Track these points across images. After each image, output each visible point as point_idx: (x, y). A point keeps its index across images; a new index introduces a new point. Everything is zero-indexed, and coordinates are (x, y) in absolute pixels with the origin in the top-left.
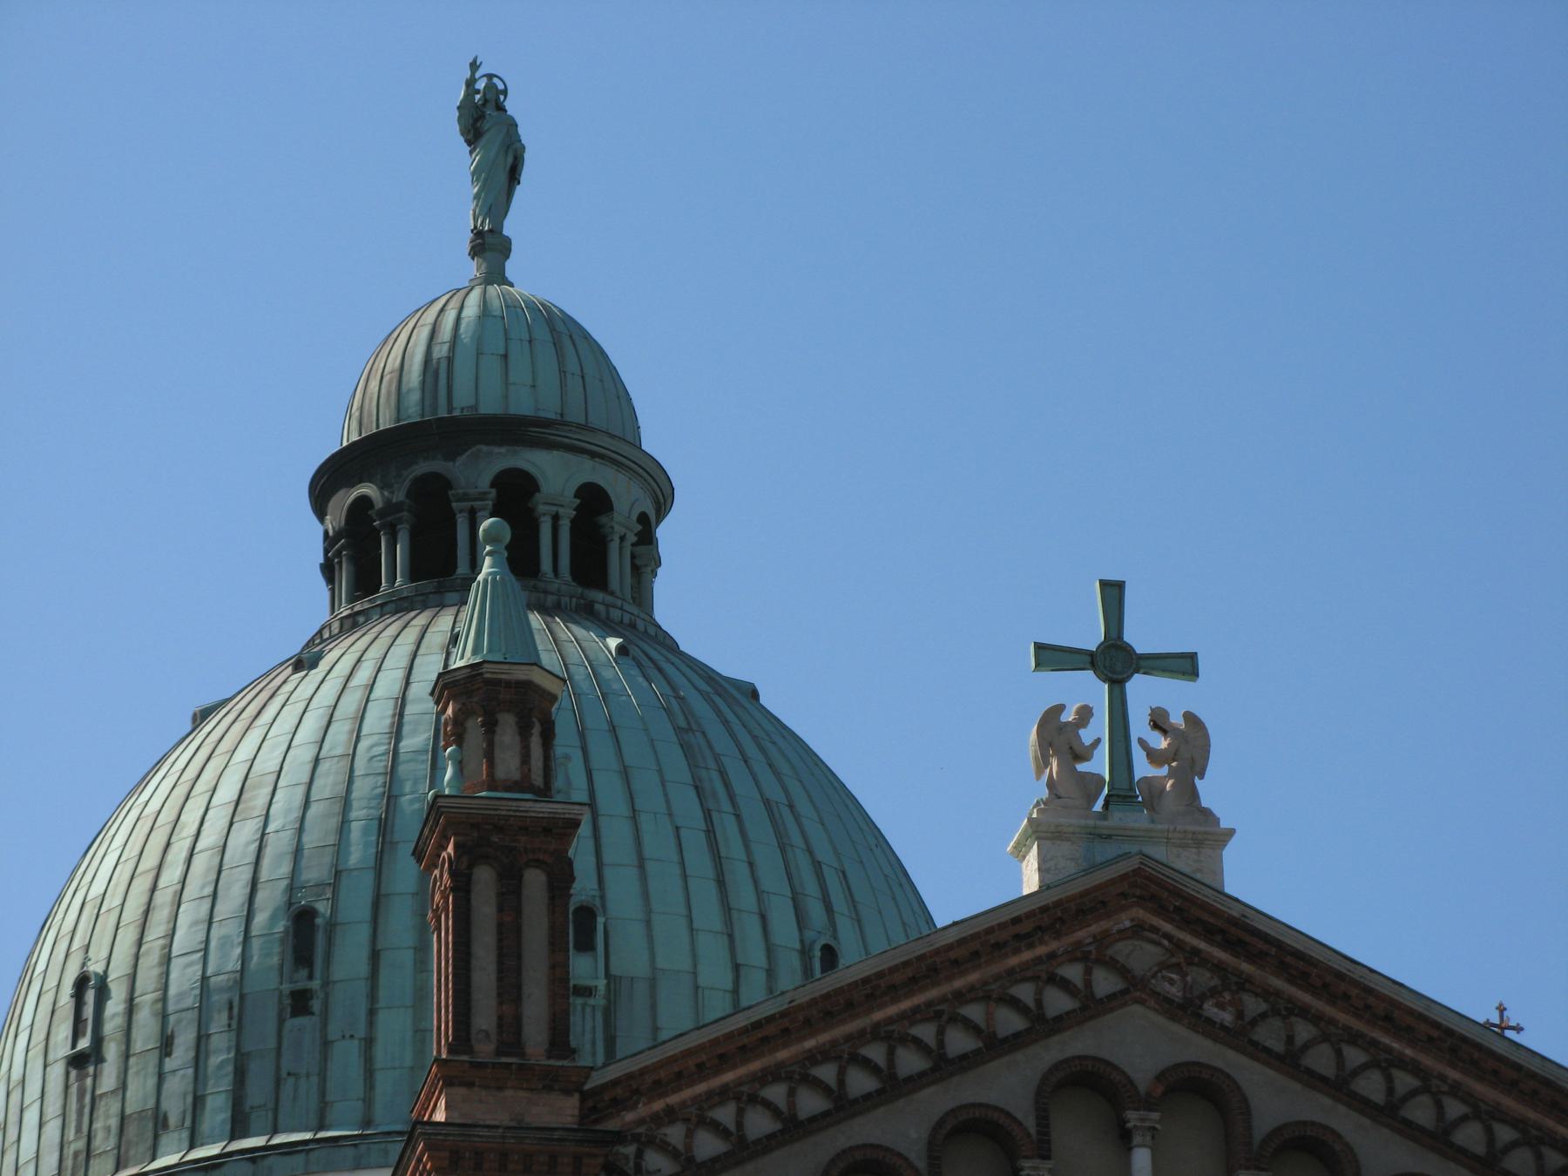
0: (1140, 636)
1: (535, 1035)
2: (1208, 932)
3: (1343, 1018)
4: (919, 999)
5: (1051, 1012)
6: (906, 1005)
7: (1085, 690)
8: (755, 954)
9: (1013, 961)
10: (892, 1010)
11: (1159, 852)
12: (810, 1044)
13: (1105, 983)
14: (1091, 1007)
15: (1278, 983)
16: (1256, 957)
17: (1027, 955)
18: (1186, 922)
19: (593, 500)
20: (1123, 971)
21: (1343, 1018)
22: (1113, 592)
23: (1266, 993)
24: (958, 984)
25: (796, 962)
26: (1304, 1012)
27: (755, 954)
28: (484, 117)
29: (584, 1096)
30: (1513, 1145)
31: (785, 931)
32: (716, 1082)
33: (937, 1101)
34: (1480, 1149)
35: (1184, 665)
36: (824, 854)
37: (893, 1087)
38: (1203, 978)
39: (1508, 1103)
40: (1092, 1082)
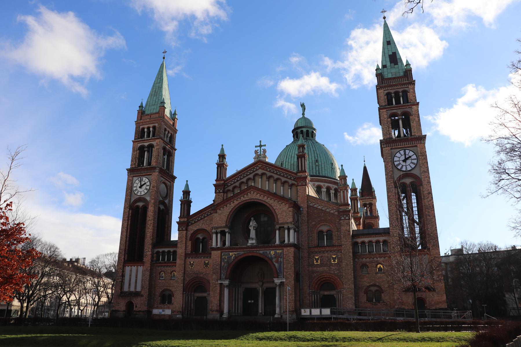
0: (262, 144)
7: (259, 148)
8: (311, 161)
11: (262, 159)
13: (258, 168)
14: (257, 170)
19: (307, 131)
22: (260, 141)
27: (311, 161)
28: (303, 106)
31: (313, 159)
33: (247, 177)
35: (265, 145)
36: (318, 153)
37: (244, 177)
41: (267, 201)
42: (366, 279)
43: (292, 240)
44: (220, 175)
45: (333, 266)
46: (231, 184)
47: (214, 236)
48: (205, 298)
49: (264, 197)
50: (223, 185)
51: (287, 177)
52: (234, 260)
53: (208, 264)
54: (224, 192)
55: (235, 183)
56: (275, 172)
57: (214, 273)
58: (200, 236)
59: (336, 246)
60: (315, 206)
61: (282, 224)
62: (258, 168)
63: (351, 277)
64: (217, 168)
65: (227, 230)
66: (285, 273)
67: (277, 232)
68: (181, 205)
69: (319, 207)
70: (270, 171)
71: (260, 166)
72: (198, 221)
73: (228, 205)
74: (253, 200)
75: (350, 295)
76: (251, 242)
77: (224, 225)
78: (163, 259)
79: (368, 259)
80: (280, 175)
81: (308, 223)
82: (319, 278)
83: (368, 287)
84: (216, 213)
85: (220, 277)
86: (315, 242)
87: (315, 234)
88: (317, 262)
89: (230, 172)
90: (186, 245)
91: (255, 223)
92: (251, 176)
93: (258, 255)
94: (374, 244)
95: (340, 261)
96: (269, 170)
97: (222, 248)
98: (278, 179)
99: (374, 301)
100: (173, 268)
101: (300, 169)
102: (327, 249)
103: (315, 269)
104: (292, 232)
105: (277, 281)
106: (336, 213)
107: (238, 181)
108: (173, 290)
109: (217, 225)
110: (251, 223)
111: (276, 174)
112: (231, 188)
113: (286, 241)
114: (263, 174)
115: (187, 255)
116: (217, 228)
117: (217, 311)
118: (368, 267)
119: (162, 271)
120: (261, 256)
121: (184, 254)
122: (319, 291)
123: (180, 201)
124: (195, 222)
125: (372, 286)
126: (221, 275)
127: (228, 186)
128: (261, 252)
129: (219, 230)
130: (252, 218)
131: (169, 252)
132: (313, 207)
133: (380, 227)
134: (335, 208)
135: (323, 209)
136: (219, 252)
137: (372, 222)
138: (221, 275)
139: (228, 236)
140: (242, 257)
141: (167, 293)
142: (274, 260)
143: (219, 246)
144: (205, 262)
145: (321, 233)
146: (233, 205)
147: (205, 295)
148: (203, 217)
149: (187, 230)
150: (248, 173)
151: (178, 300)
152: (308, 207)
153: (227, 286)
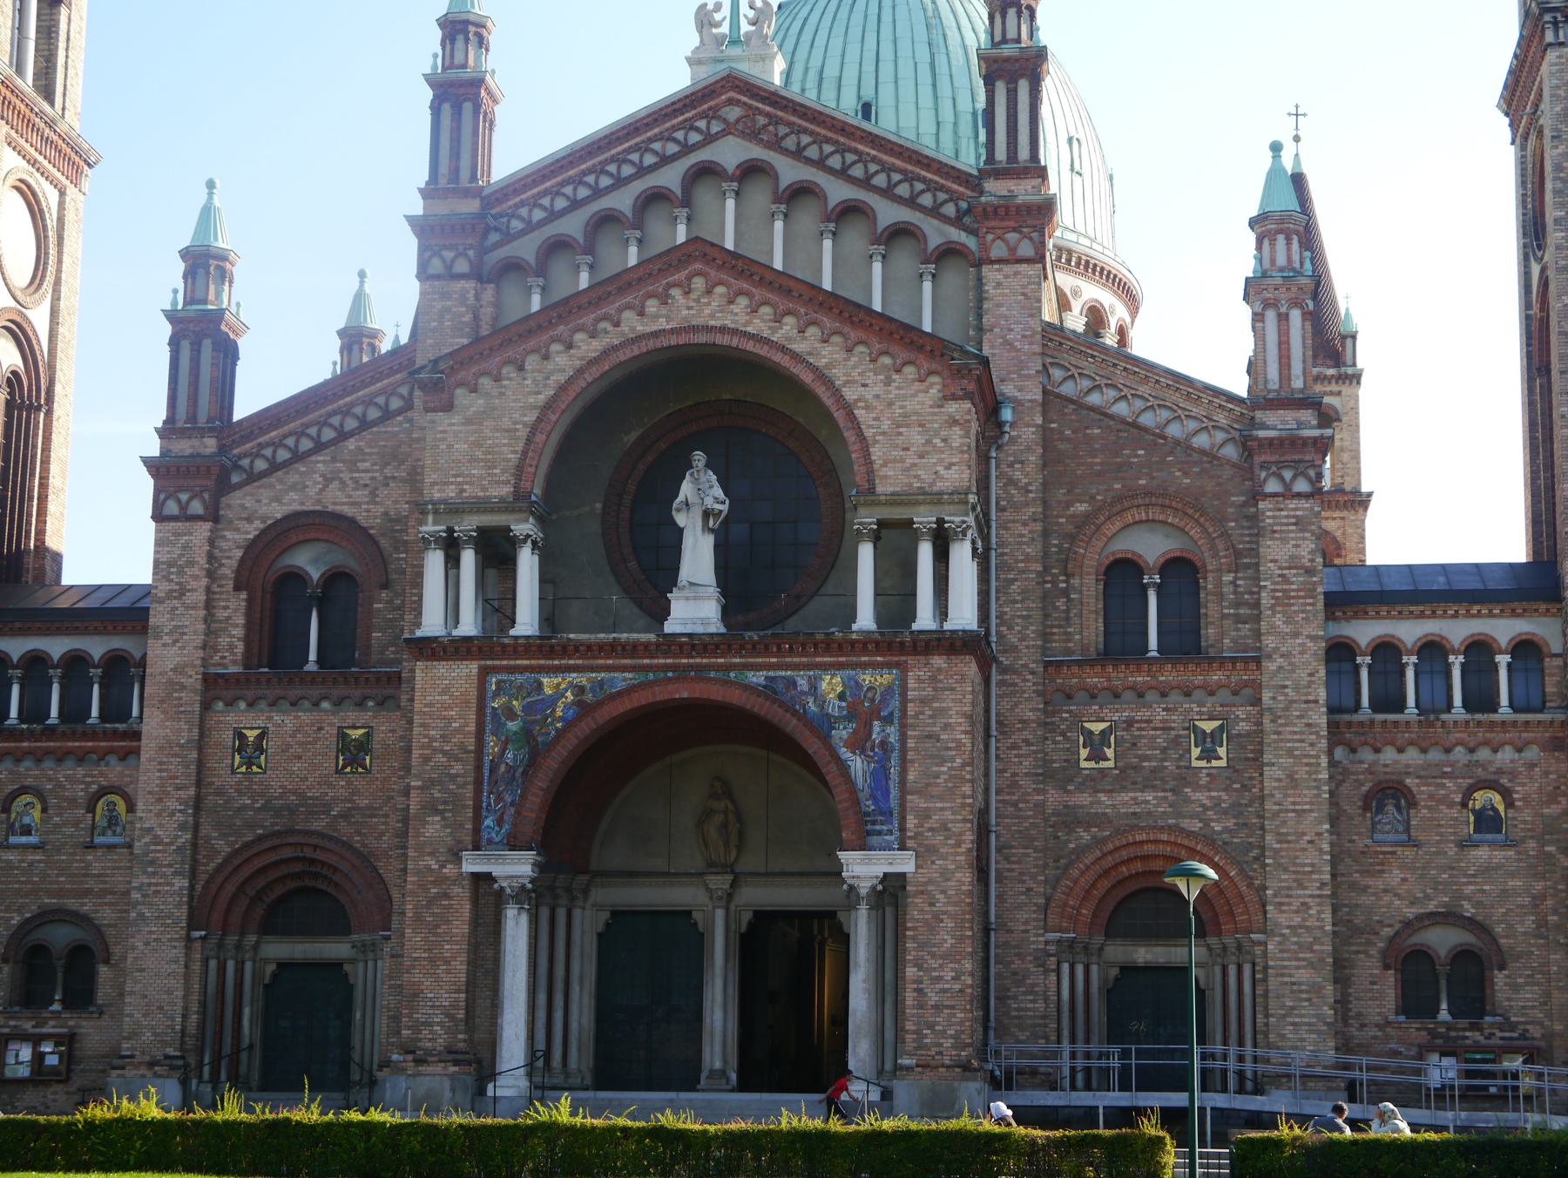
1: (465, 174)
2: (763, 100)
3: (823, 132)
4: (632, 143)
5: (691, 142)
6: (626, 145)
9: (675, 122)
10: (620, 149)
12: (583, 167)
14: (709, 139)
15: (793, 119)
16: (784, 108)
17: (681, 118)
18: (754, 96)
20: (725, 120)
21: (823, 132)
23: (789, 124)
24: (649, 134)
25: (969, 118)
26: (805, 131)
29: (482, 199)
30: (900, 182)
32: (542, 187)
33: (638, 186)
34: (884, 185)
37: (620, 182)
38: (762, 120)
39: (898, 163)
40: (706, 171)
41: (799, 347)
42: (1395, 876)
43: (964, 614)
44: (455, 155)
45: (1197, 788)
46: (531, 227)
47: (435, 562)
48: (335, 966)
49: (778, 319)
50: (468, 224)
51: (911, 202)
52: (569, 724)
53: (364, 746)
54: (477, 275)
55: (554, 215)
56: (835, 162)
57: (431, 808)
58: (310, 562)
59: (1222, 661)
60: (1095, 399)
61: (895, 500)
62: (716, 128)
63: (1316, 859)
64: (436, 109)
65: (524, 527)
66: (911, 822)
67: (866, 554)
68: (174, 343)
69: (1121, 409)
70: (798, 154)
71: (734, 113)
72: (297, 457)
73: (532, 362)
74: (703, 338)
75: (1303, 975)
76: (695, 608)
77: (506, 490)
78: (34, 710)
79: (1412, 756)
80: (865, 183)
81: (1045, 504)
82: (1109, 861)
83: (1408, 924)
84: (448, 407)
85: (477, 831)
86: (1090, 630)
87: (1090, 580)
88: (1097, 756)
89: (519, 143)
90: (209, 619)
91: (718, 492)
92: (671, 178)
93: (736, 698)
94: (1456, 661)
95: (1251, 754)
96: (790, 143)
97: (491, 647)
98: (850, 210)
99: (1444, 1015)
100: (114, 771)
101: (1001, 154)
102: (1167, 676)
103: (1084, 799)
104: (962, 559)
105: (862, 868)
106: (1230, 452)
107: (575, 204)
108: (106, 916)
109: (451, 492)
110: (686, 489)
111: (842, 174)
112: (527, 249)
113: (925, 619)
114: (751, 171)
115: (215, 686)
116: (455, 509)
117: (452, 1055)
118: (1412, 803)
119: (23, 790)
120: (760, 707)
121: (193, 679)
122: (1098, 940)
123: (171, 316)
124: (275, 467)
125: (1434, 919)
126: (477, 819)
127: (509, 237)
128: (757, 678)
129: (468, 525)
130: (699, 458)
131: (75, 663)
132: (1076, 403)
133: (1372, 559)
134: (1222, 419)
135: (1147, 419)
136: (473, 667)
137: (1329, 525)
138: (477, 819)
139: (527, 565)
140: (626, 705)
141: (60, 937)
142: (841, 734)
143: (468, 626)
144: (342, 736)
145: (1123, 572)
146: (563, 364)
147: (335, 949)
148: (328, 434)
149: (213, 515)
150: (649, 159)
151: (155, 978)
152: (1050, 398)
153: (521, 895)
